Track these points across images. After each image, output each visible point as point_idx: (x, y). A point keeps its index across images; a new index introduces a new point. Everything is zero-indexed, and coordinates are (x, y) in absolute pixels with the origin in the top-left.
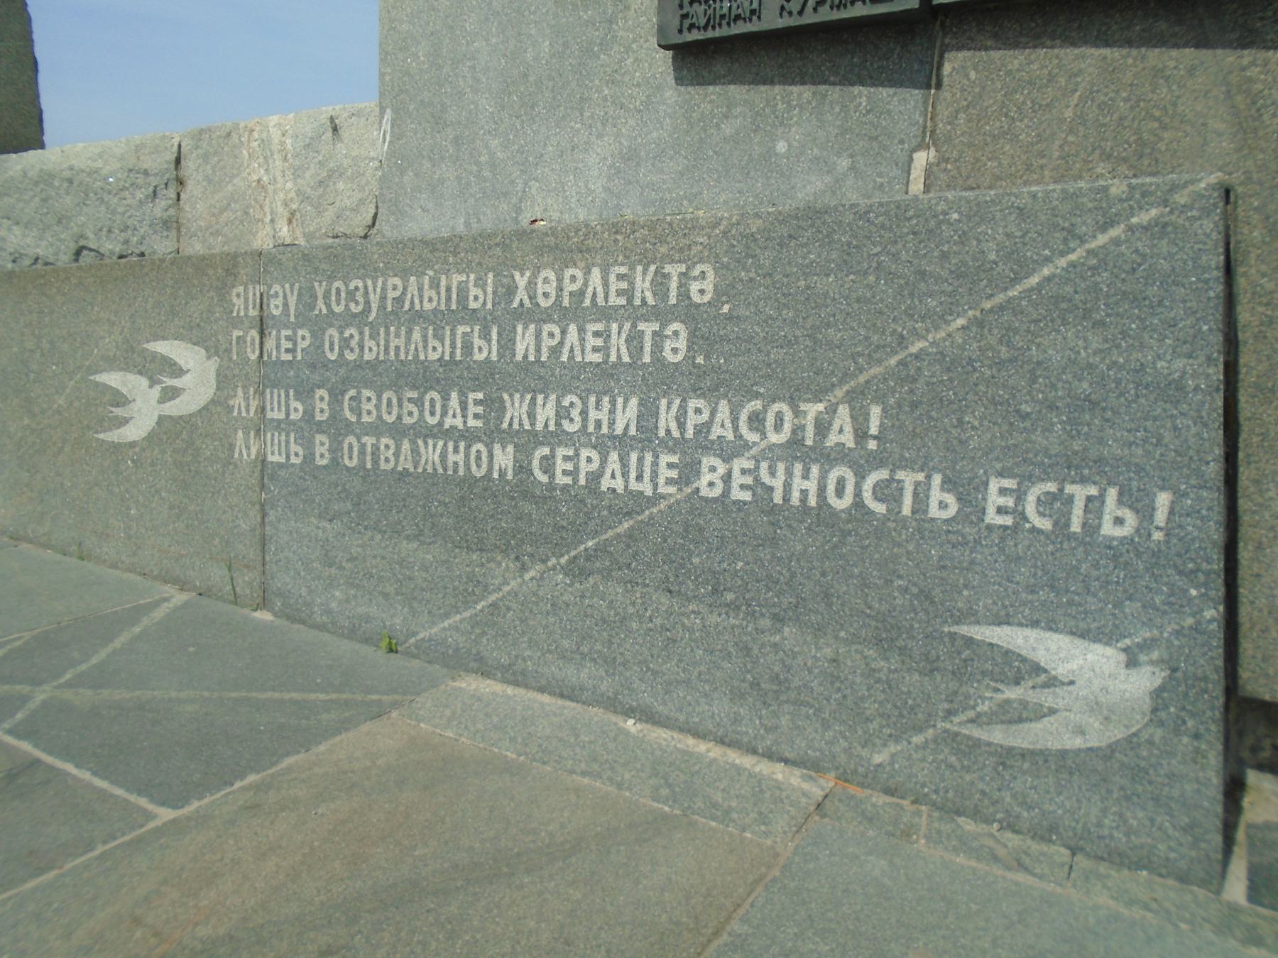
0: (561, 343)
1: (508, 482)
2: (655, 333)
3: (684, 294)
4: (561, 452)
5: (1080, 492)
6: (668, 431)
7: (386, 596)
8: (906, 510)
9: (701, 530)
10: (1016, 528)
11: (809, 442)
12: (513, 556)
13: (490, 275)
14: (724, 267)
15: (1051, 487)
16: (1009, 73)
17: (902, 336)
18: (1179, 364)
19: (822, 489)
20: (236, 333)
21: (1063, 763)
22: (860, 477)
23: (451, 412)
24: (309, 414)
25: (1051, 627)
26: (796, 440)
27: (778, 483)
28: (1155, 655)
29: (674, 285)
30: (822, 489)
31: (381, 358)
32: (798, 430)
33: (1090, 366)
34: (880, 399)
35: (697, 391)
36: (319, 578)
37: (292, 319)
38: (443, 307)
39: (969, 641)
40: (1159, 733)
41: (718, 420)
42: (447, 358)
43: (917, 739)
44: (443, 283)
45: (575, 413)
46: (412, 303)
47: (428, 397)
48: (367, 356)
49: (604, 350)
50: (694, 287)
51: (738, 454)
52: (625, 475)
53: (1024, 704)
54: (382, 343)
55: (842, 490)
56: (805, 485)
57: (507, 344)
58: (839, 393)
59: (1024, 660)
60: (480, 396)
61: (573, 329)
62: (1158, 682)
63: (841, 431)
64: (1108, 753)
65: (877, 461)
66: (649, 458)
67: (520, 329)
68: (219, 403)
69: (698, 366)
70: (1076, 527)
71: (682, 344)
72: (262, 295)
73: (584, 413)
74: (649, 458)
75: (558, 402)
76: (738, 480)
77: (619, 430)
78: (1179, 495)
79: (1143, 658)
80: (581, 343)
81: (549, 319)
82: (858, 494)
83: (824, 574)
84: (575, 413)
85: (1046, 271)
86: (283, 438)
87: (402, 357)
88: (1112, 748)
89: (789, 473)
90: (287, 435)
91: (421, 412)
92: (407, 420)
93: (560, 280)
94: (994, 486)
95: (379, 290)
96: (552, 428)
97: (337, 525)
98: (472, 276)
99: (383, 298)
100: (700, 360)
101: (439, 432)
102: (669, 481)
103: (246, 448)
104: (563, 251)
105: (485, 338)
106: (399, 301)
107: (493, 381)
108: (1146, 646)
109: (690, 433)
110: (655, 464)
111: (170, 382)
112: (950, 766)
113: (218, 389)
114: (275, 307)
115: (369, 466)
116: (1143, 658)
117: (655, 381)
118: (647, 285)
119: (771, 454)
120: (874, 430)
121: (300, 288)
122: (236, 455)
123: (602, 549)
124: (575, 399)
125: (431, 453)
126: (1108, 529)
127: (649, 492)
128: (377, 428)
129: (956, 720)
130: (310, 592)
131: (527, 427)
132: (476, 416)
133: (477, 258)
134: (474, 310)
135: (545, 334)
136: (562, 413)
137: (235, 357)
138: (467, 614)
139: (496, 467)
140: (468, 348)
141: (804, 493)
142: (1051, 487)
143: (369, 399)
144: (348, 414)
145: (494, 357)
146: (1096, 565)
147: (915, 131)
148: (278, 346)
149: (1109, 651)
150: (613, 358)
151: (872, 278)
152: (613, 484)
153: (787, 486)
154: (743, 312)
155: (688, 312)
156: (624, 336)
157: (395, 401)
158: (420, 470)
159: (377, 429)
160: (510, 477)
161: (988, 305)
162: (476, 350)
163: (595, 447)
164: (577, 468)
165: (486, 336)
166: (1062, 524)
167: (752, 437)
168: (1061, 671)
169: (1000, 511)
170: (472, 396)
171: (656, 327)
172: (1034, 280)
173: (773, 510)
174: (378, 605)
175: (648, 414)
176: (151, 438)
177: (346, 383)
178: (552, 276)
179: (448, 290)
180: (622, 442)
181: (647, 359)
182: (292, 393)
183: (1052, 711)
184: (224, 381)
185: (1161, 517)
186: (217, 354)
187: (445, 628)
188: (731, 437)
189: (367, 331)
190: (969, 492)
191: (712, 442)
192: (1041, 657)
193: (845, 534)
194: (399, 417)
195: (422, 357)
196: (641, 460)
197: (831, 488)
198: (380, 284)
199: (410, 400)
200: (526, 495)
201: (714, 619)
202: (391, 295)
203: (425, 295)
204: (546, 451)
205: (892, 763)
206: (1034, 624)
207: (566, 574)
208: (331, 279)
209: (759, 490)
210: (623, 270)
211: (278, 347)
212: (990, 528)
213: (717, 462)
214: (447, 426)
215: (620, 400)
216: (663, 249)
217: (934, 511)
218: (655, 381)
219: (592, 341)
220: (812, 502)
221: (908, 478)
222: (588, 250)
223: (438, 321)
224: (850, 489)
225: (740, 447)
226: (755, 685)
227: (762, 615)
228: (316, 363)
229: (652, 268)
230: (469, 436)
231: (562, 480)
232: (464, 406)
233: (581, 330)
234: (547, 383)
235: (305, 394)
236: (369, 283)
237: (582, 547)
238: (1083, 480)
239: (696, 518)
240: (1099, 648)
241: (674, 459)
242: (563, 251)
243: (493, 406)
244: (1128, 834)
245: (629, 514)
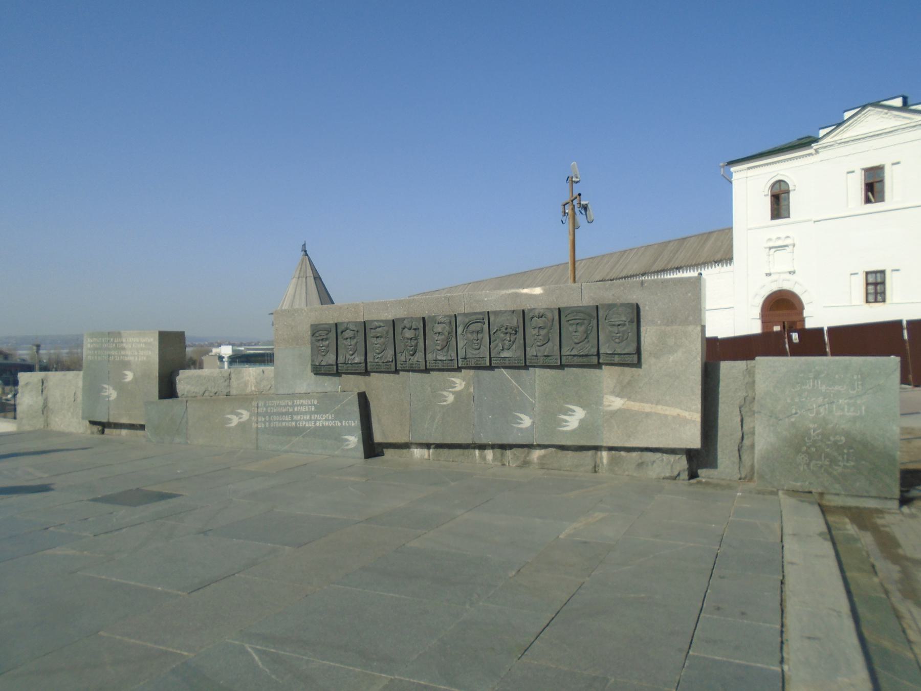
21: (351, 449)
55: (331, 424)
56: (326, 424)
68: (250, 419)
80: (303, 409)
103: (254, 426)
107: (292, 414)
117: (311, 413)
125: (284, 424)
148: (260, 410)
176: (236, 426)
184: (251, 416)
187: (286, 448)
203: (283, 403)
218: (311, 413)
223: (285, 406)
228: (266, 412)
235: (265, 417)
243: (292, 417)
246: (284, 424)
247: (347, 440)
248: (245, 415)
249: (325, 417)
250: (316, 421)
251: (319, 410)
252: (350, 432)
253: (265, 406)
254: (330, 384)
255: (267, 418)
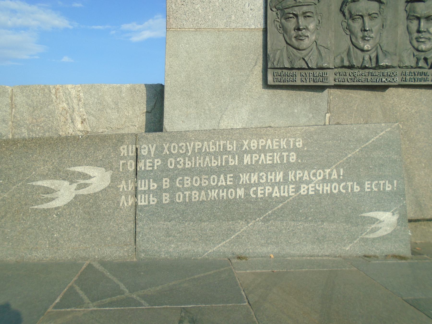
0: (259, 159)
1: (242, 199)
2: (287, 155)
3: (294, 145)
4: (259, 188)
5: (382, 182)
6: (292, 180)
7: (195, 242)
8: (350, 191)
9: (302, 203)
10: (371, 191)
11: (327, 178)
12: (244, 220)
13: (235, 141)
14: (305, 139)
15: (377, 182)
16: (344, 99)
17: (346, 154)
18: (396, 156)
19: (331, 189)
20: (122, 162)
21: (383, 238)
22: (339, 185)
23: (221, 181)
24: (160, 188)
25: (379, 210)
26: (324, 178)
27: (321, 189)
28: (397, 212)
29: (292, 143)
30: (331, 189)
31: (193, 166)
32: (324, 176)
33: (381, 158)
34: (343, 167)
35: (299, 169)
36: (164, 242)
37: (152, 156)
38: (217, 150)
39: (364, 217)
40: (399, 227)
41: (305, 175)
42: (219, 165)
43: (355, 242)
44: (217, 144)
45: (264, 178)
46: (206, 149)
47: (212, 177)
48: (187, 166)
49: (273, 160)
50: (297, 144)
51: (311, 183)
52: (280, 192)
53: (376, 228)
54: (193, 162)
55: (335, 188)
56: (327, 188)
57: (241, 160)
58: (334, 167)
59: (375, 218)
60: (232, 175)
61: (263, 155)
62: (398, 217)
63: (334, 175)
64: (391, 234)
65: (343, 181)
66: (286, 187)
67: (245, 156)
69: (299, 163)
70: (381, 189)
71: (295, 157)
72: (137, 149)
73: (267, 177)
74: (286, 187)
75: (258, 174)
76: (311, 189)
77: (277, 180)
78: (398, 181)
79: (395, 213)
81: (255, 152)
82: (339, 189)
83: (333, 209)
84: (264, 178)
85: (373, 140)
86: (147, 196)
87: (202, 165)
88: (392, 232)
89: (323, 186)
90: (149, 195)
91: (209, 182)
92: (203, 185)
93: (258, 142)
94: (366, 183)
95: (192, 146)
96: (256, 182)
97: (173, 222)
98: (228, 142)
99: (194, 148)
100: (299, 161)
101: (217, 187)
102: (292, 192)
104: (259, 135)
105: (234, 159)
106: (201, 149)
107: (236, 171)
108: (396, 210)
109: (297, 179)
110: (288, 188)
111: (82, 182)
112: (363, 246)
113: (111, 182)
114: (144, 152)
115: (187, 201)
116: (395, 213)
117: (288, 167)
118: (284, 143)
119: (319, 182)
120: (341, 174)
121: (157, 146)
122: (121, 205)
123: (274, 213)
124: (264, 174)
126: (387, 189)
127: (287, 195)
128: (191, 188)
129: (363, 235)
130: (159, 247)
131: (248, 182)
132: (230, 181)
133: (230, 137)
134: (229, 151)
135: (254, 157)
136: (259, 178)
137: (121, 170)
138: (228, 241)
139: (238, 195)
140: (227, 162)
141: (327, 190)
142: (377, 182)
143: (188, 180)
144: (178, 185)
145: (236, 164)
146: (386, 197)
147: (326, 109)
149: (390, 213)
150: (275, 162)
151: (339, 141)
152: (276, 195)
153: (323, 189)
154: (310, 149)
155: (296, 150)
156: (278, 156)
157: (199, 179)
158: (209, 199)
159: (191, 189)
160: (243, 197)
161: (363, 146)
162: (230, 162)
163: (270, 186)
164: (265, 192)
165: (234, 158)
166: (379, 189)
167: (314, 179)
168: (382, 219)
169: (368, 188)
170: (228, 176)
171: (287, 154)
172: (371, 142)
173: (320, 195)
174: (191, 245)
175: (286, 175)
177: (177, 176)
178: (256, 142)
179: (219, 145)
180: (279, 184)
181: (285, 162)
182: (151, 180)
183: (381, 228)
184: (114, 179)
185: (395, 185)
186: (111, 169)
188: (308, 179)
189: (187, 159)
190: (361, 185)
191: (304, 181)
192: (378, 217)
193: (337, 198)
194: (201, 184)
195: (210, 165)
196: (284, 188)
197: (333, 188)
198: (192, 144)
199: (205, 179)
200: (248, 202)
201: (306, 225)
202: (197, 147)
204: (255, 188)
205: (350, 249)
206: (376, 211)
207: (262, 222)
208: (171, 143)
209: (316, 191)
210: (277, 140)
211: (145, 166)
212: (367, 192)
213: (305, 185)
214: (219, 185)
215: (278, 173)
216: (289, 135)
217: (355, 190)
218: (289, 166)
219: (268, 158)
220: (329, 192)
221: (349, 184)
222: (267, 135)
223: (216, 155)
224: (337, 188)
225: (311, 181)
226: (318, 239)
227: (319, 221)
228: (164, 170)
229: (286, 139)
230: (228, 187)
231: (260, 196)
232: (226, 179)
233: (265, 155)
234: (255, 170)
236: (188, 144)
237: (267, 214)
238: (382, 180)
239: (300, 200)
240: (388, 213)
241: (293, 186)
242: (259, 135)
243: (236, 178)
244: (396, 249)
245: (281, 202)
246: (213, 194)
247: (375, 220)
248: (98, 179)
249: (321, 174)
250: (298, 184)
251: (308, 160)
252: (381, 202)
253: (159, 153)
254: (301, 111)
255: (166, 183)
